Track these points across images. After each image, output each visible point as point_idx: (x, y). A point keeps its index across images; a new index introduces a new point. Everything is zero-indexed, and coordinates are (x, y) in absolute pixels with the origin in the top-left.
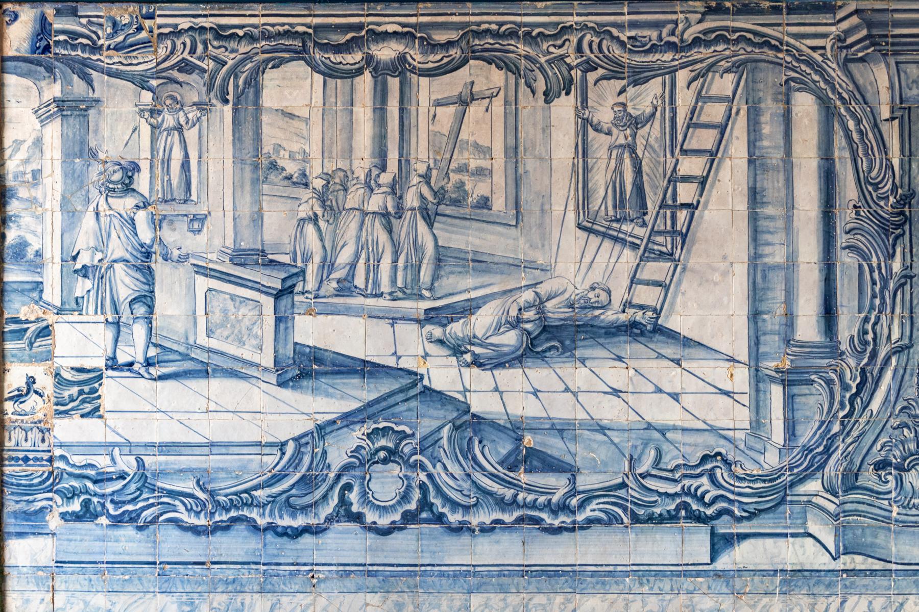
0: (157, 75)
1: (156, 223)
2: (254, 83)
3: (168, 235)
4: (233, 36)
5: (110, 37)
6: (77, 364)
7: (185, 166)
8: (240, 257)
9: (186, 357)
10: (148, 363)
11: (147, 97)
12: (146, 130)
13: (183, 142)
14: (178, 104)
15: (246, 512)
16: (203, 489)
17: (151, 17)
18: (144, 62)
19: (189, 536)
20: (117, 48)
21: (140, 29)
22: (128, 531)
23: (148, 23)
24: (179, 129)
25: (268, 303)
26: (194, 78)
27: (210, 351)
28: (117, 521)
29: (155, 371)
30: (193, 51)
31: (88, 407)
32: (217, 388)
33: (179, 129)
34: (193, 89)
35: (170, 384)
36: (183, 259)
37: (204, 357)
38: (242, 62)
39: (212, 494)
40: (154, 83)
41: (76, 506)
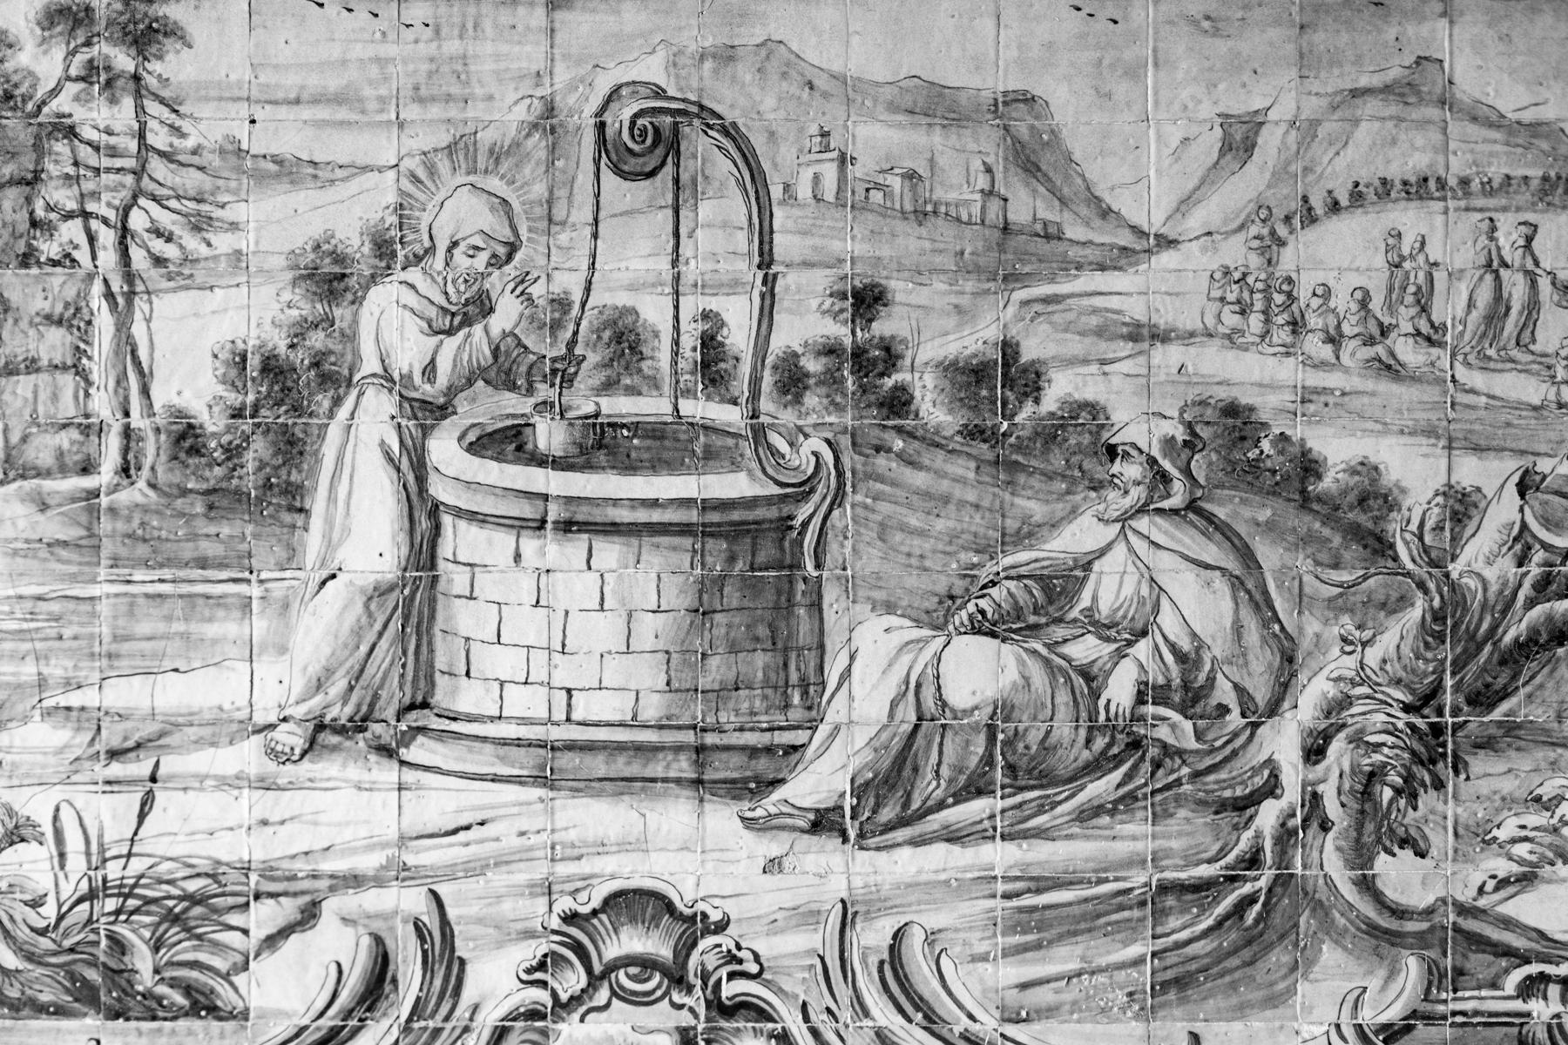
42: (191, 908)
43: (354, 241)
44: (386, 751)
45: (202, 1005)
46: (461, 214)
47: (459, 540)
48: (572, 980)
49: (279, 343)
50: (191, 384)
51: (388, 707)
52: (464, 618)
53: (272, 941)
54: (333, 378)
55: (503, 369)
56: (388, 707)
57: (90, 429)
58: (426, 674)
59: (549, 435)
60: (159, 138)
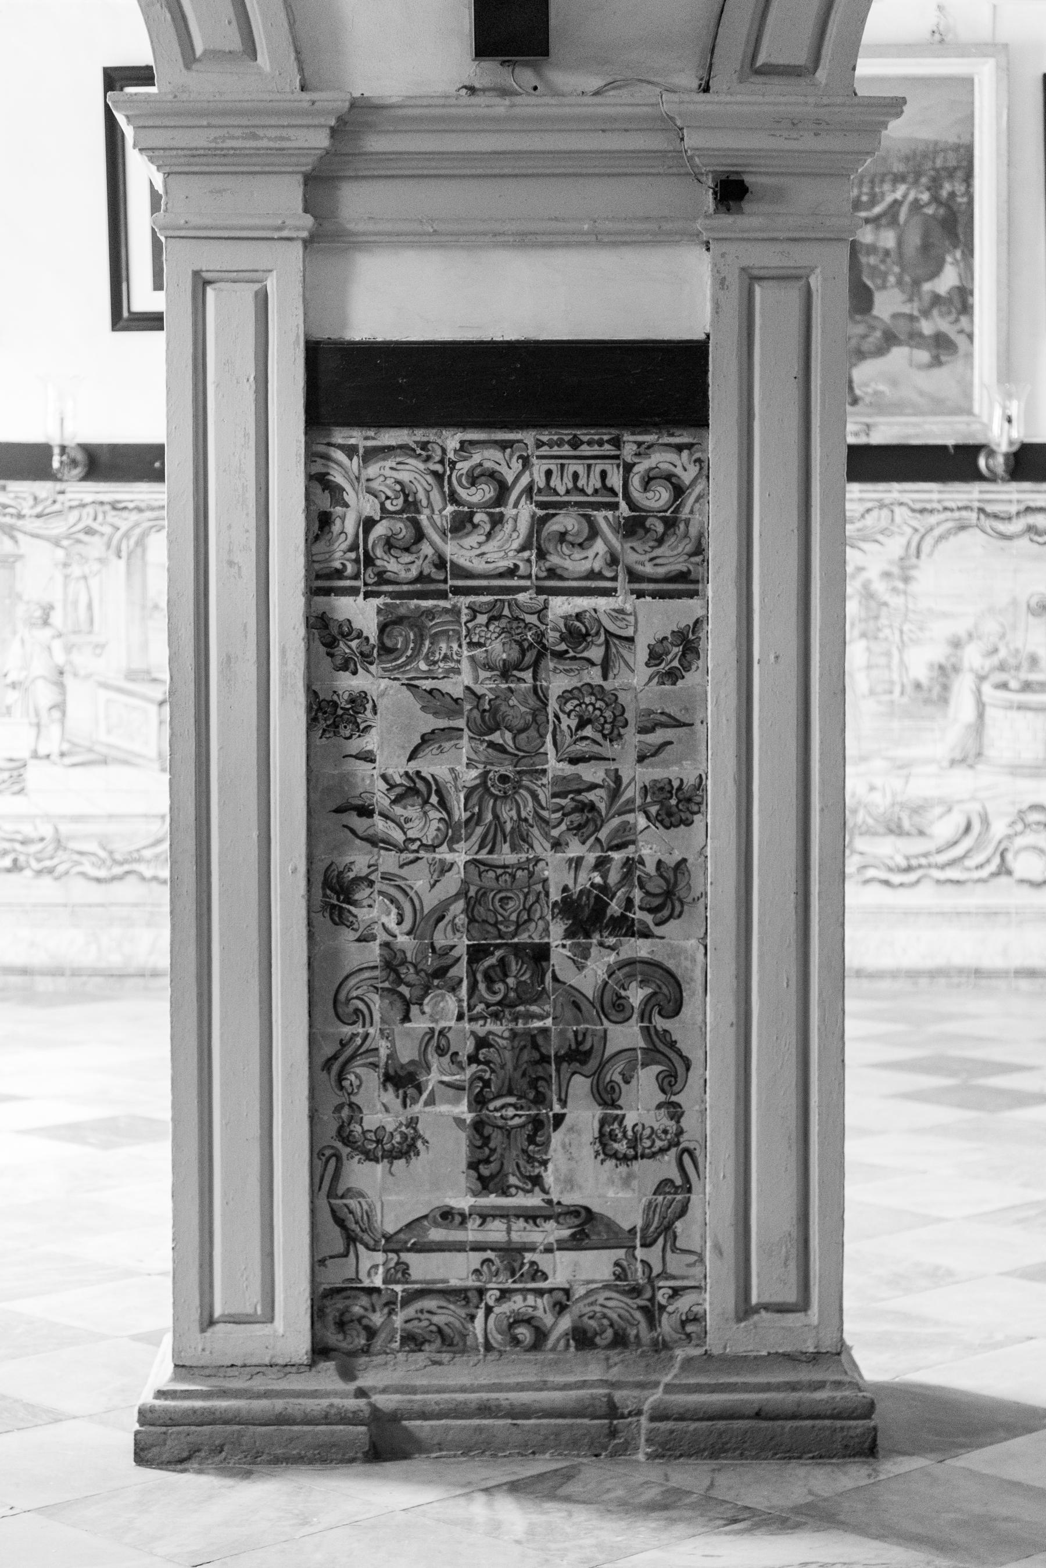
0: (68, 537)
1: (69, 649)
2: (141, 542)
3: (77, 658)
4: (125, 508)
5: (32, 507)
6: (9, 755)
7: (90, 606)
8: (131, 676)
9: (90, 750)
10: (62, 755)
11: (60, 554)
12: (59, 578)
13: (88, 588)
14: (84, 559)
15: (135, 867)
16: (104, 849)
17: (62, 492)
18: (57, 527)
19: (94, 885)
20: (39, 516)
21: (54, 502)
22: (47, 880)
23: (60, 498)
24: (85, 578)
25: (153, 709)
26: (95, 539)
27: (109, 746)
28: (39, 873)
29: (67, 760)
30: (95, 519)
31: (16, 788)
32: (113, 771)
33: (85, 578)
34: (95, 546)
35: (79, 770)
36: (88, 676)
37: (104, 750)
38: (132, 528)
39: (111, 853)
40: (65, 543)
41: (7, 862)
42: (918, 809)
43: (963, 635)
44: (971, 767)
45: (921, 833)
46: (991, 627)
47: (990, 712)
48: (1019, 827)
49: (943, 661)
50: (920, 671)
51: (970, 756)
52: (991, 732)
53: (941, 817)
54: (956, 669)
55: (1002, 667)
56: (970, 756)
57: (892, 683)
58: (981, 747)
59: (1014, 684)
60: (911, 606)
